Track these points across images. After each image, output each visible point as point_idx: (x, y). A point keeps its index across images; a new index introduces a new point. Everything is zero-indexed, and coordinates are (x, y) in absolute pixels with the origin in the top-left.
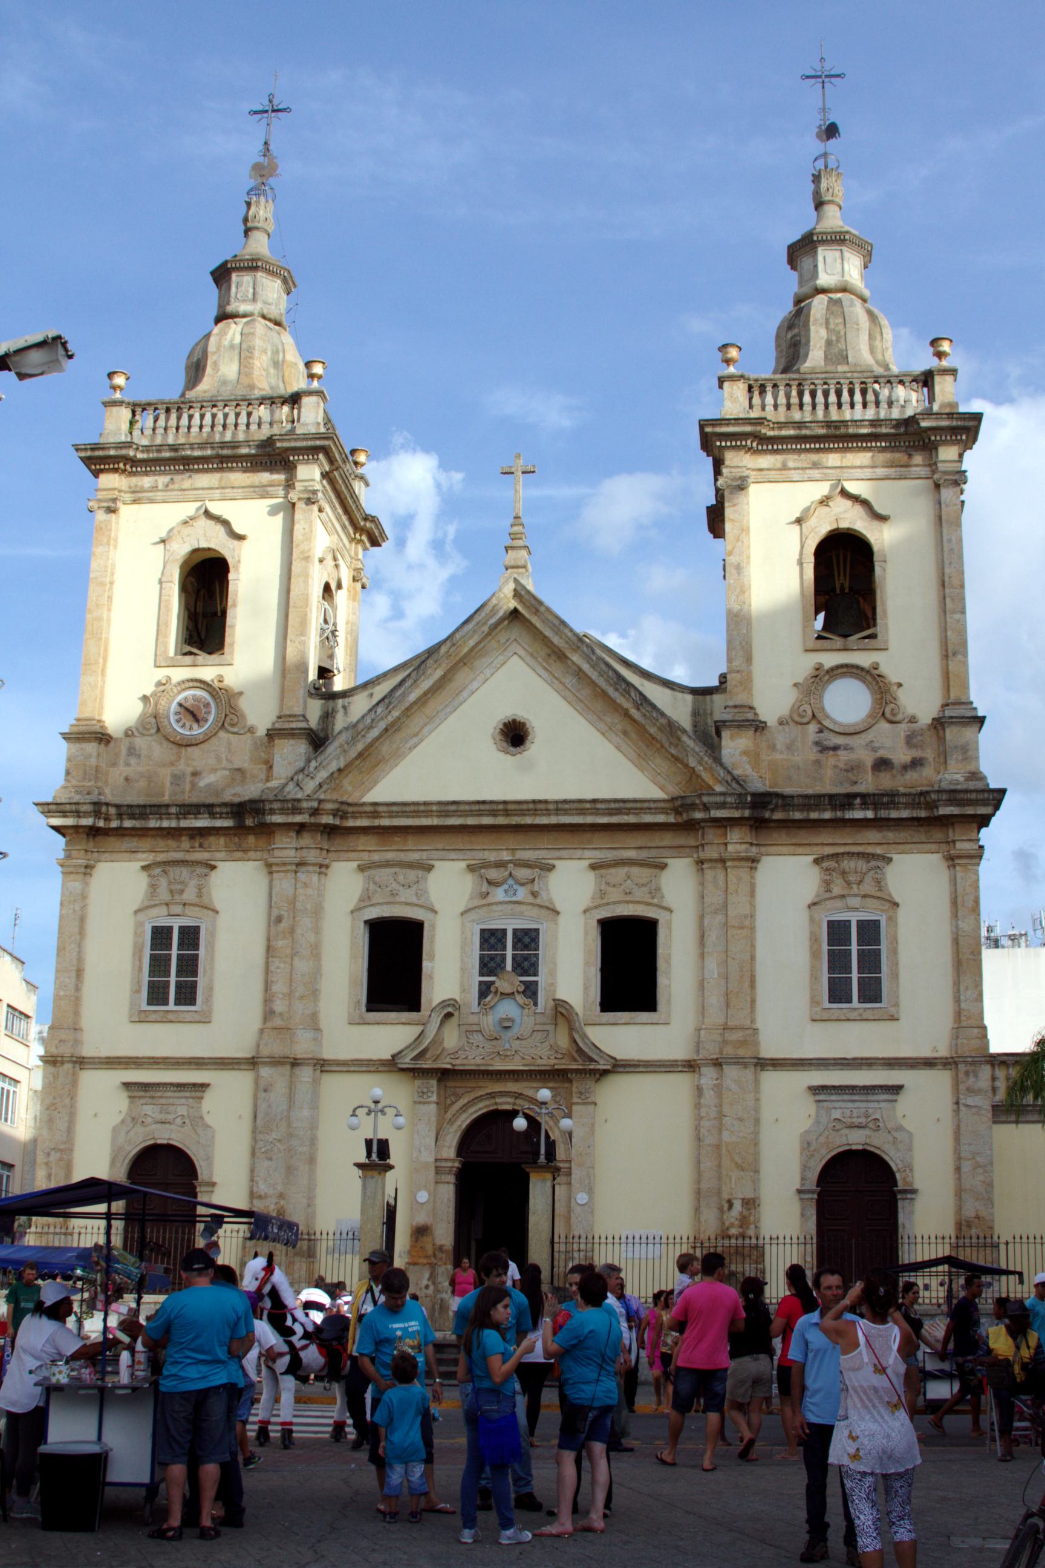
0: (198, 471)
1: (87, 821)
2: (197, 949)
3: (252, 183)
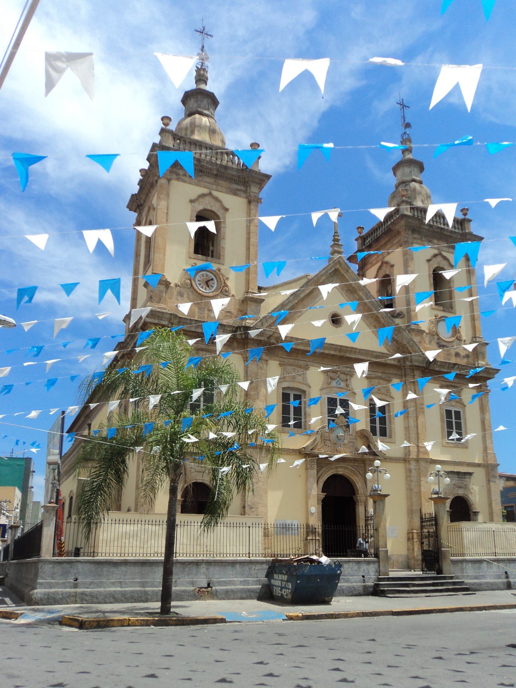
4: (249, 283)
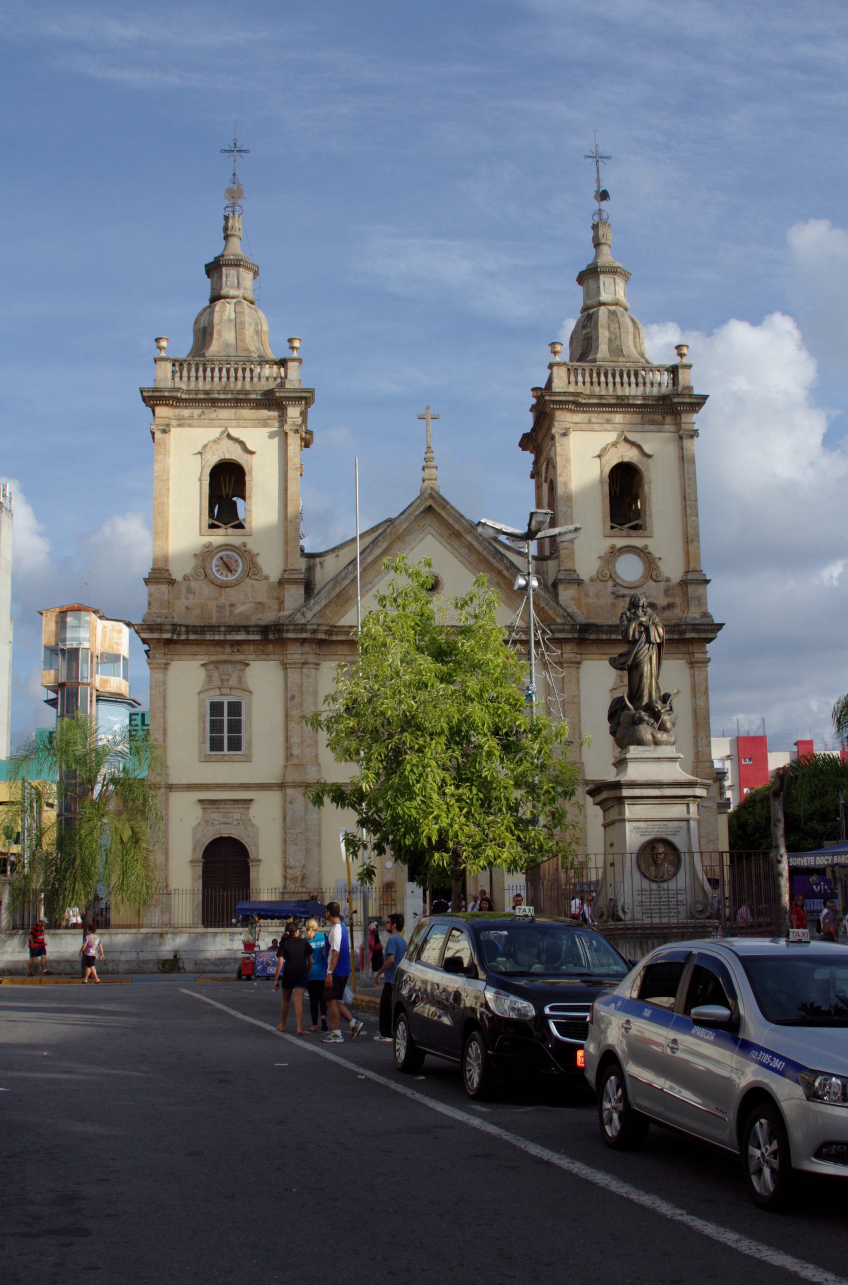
0: (221, 407)
1: (167, 636)
2: (240, 716)
3: (227, 202)
4: (287, 557)
